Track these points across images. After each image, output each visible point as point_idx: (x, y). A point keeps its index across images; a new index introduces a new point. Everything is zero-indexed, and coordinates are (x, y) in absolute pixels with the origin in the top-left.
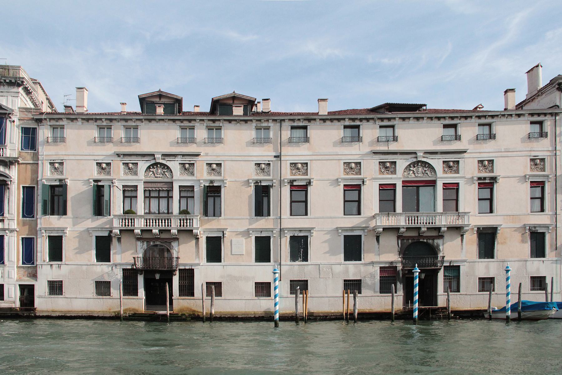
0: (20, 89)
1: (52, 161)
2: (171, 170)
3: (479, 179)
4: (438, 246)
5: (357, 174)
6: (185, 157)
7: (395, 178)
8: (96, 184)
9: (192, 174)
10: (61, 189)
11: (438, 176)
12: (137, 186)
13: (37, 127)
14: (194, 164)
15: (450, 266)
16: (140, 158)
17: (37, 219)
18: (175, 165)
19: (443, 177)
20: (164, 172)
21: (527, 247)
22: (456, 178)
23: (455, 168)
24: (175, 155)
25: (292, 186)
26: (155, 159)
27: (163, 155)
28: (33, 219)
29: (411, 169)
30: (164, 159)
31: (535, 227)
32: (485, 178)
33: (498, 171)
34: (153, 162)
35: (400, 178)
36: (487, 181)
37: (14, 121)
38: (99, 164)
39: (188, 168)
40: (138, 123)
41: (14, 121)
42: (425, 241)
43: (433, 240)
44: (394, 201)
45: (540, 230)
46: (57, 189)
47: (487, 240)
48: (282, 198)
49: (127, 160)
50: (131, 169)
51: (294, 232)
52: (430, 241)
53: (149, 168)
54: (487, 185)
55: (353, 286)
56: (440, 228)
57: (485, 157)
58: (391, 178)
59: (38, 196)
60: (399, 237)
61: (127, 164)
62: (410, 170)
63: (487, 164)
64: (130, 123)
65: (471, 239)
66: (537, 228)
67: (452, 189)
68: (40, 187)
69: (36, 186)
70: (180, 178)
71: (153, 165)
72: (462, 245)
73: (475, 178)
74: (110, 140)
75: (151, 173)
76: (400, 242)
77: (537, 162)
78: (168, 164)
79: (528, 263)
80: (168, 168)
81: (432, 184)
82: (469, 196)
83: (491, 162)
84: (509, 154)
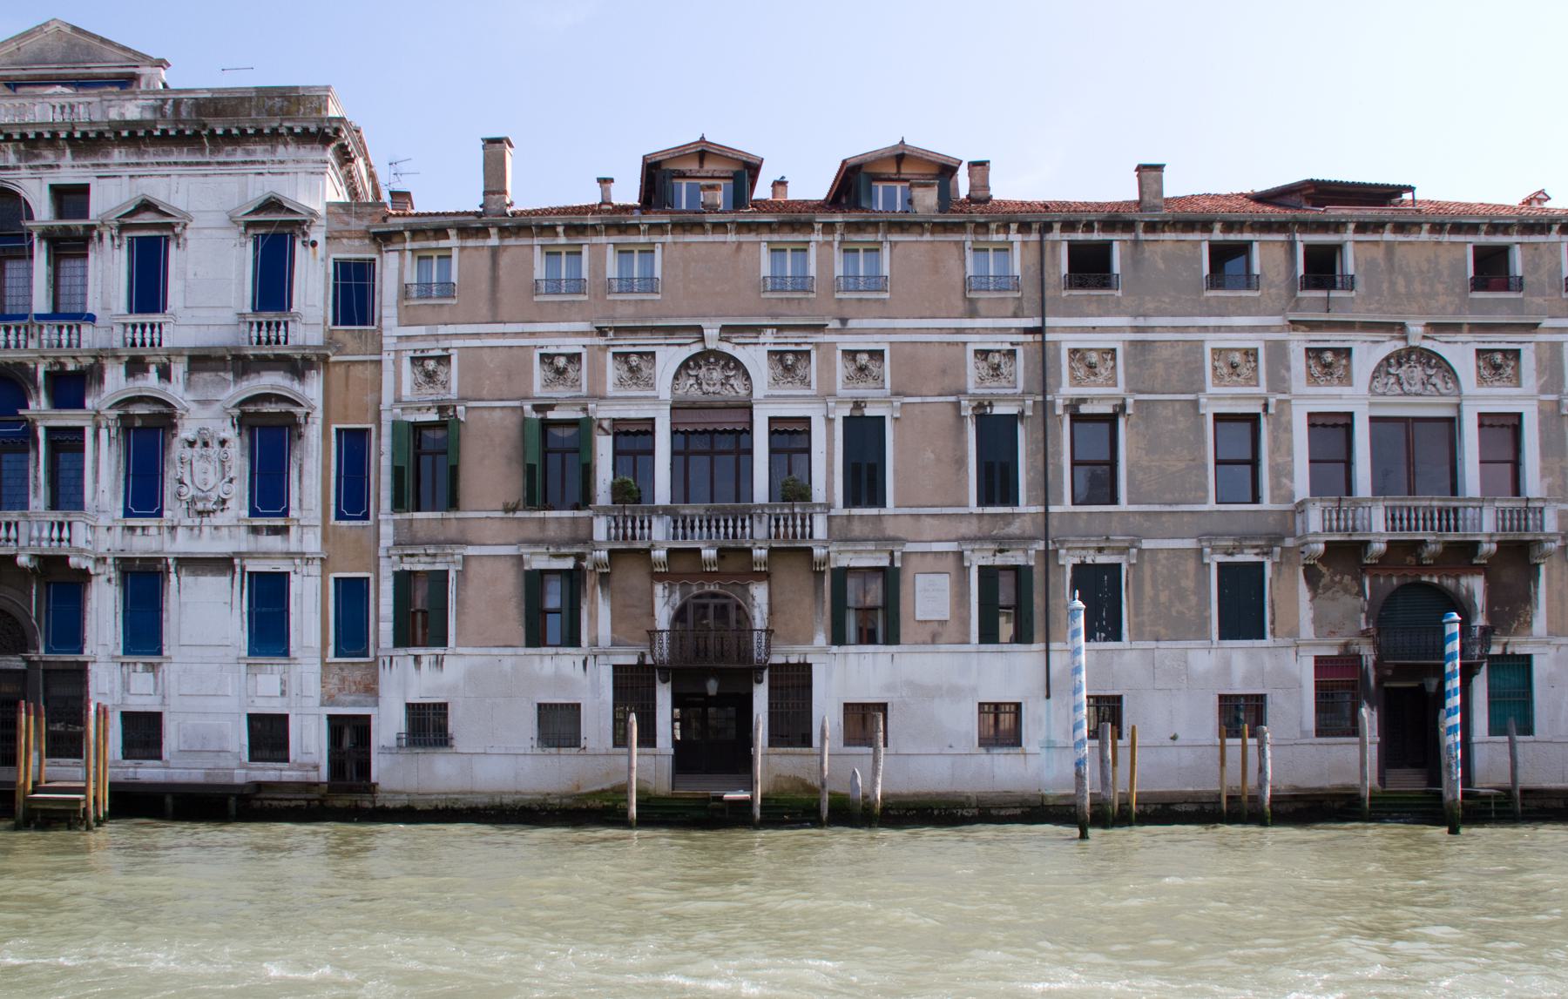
0: (329, 154)
1: (418, 354)
4: (1471, 594)
5: (1247, 385)
6: (786, 334)
8: (540, 416)
9: (805, 382)
10: (439, 434)
12: (653, 419)
13: (377, 256)
14: (808, 353)
15: (1504, 656)
17: (378, 522)
18: (755, 357)
20: (728, 378)
23: (1509, 371)
26: (702, 340)
27: (724, 328)
28: (366, 523)
29: (1392, 370)
30: (727, 340)
34: (697, 348)
37: (314, 244)
41: (314, 244)
42: (1436, 580)
43: (1457, 577)
44: (1348, 463)
46: (429, 434)
49: (625, 344)
51: (1084, 553)
53: (685, 365)
56: (1479, 542)
58: (1340, 397)
59: (380, 454)
61: (627, 355)
62: (1388, 373)
68: (386, 430)
69: (373, 426)
71: (693, 357)
75: (692, 381)
78: (738, 353)
80: (739, 365)
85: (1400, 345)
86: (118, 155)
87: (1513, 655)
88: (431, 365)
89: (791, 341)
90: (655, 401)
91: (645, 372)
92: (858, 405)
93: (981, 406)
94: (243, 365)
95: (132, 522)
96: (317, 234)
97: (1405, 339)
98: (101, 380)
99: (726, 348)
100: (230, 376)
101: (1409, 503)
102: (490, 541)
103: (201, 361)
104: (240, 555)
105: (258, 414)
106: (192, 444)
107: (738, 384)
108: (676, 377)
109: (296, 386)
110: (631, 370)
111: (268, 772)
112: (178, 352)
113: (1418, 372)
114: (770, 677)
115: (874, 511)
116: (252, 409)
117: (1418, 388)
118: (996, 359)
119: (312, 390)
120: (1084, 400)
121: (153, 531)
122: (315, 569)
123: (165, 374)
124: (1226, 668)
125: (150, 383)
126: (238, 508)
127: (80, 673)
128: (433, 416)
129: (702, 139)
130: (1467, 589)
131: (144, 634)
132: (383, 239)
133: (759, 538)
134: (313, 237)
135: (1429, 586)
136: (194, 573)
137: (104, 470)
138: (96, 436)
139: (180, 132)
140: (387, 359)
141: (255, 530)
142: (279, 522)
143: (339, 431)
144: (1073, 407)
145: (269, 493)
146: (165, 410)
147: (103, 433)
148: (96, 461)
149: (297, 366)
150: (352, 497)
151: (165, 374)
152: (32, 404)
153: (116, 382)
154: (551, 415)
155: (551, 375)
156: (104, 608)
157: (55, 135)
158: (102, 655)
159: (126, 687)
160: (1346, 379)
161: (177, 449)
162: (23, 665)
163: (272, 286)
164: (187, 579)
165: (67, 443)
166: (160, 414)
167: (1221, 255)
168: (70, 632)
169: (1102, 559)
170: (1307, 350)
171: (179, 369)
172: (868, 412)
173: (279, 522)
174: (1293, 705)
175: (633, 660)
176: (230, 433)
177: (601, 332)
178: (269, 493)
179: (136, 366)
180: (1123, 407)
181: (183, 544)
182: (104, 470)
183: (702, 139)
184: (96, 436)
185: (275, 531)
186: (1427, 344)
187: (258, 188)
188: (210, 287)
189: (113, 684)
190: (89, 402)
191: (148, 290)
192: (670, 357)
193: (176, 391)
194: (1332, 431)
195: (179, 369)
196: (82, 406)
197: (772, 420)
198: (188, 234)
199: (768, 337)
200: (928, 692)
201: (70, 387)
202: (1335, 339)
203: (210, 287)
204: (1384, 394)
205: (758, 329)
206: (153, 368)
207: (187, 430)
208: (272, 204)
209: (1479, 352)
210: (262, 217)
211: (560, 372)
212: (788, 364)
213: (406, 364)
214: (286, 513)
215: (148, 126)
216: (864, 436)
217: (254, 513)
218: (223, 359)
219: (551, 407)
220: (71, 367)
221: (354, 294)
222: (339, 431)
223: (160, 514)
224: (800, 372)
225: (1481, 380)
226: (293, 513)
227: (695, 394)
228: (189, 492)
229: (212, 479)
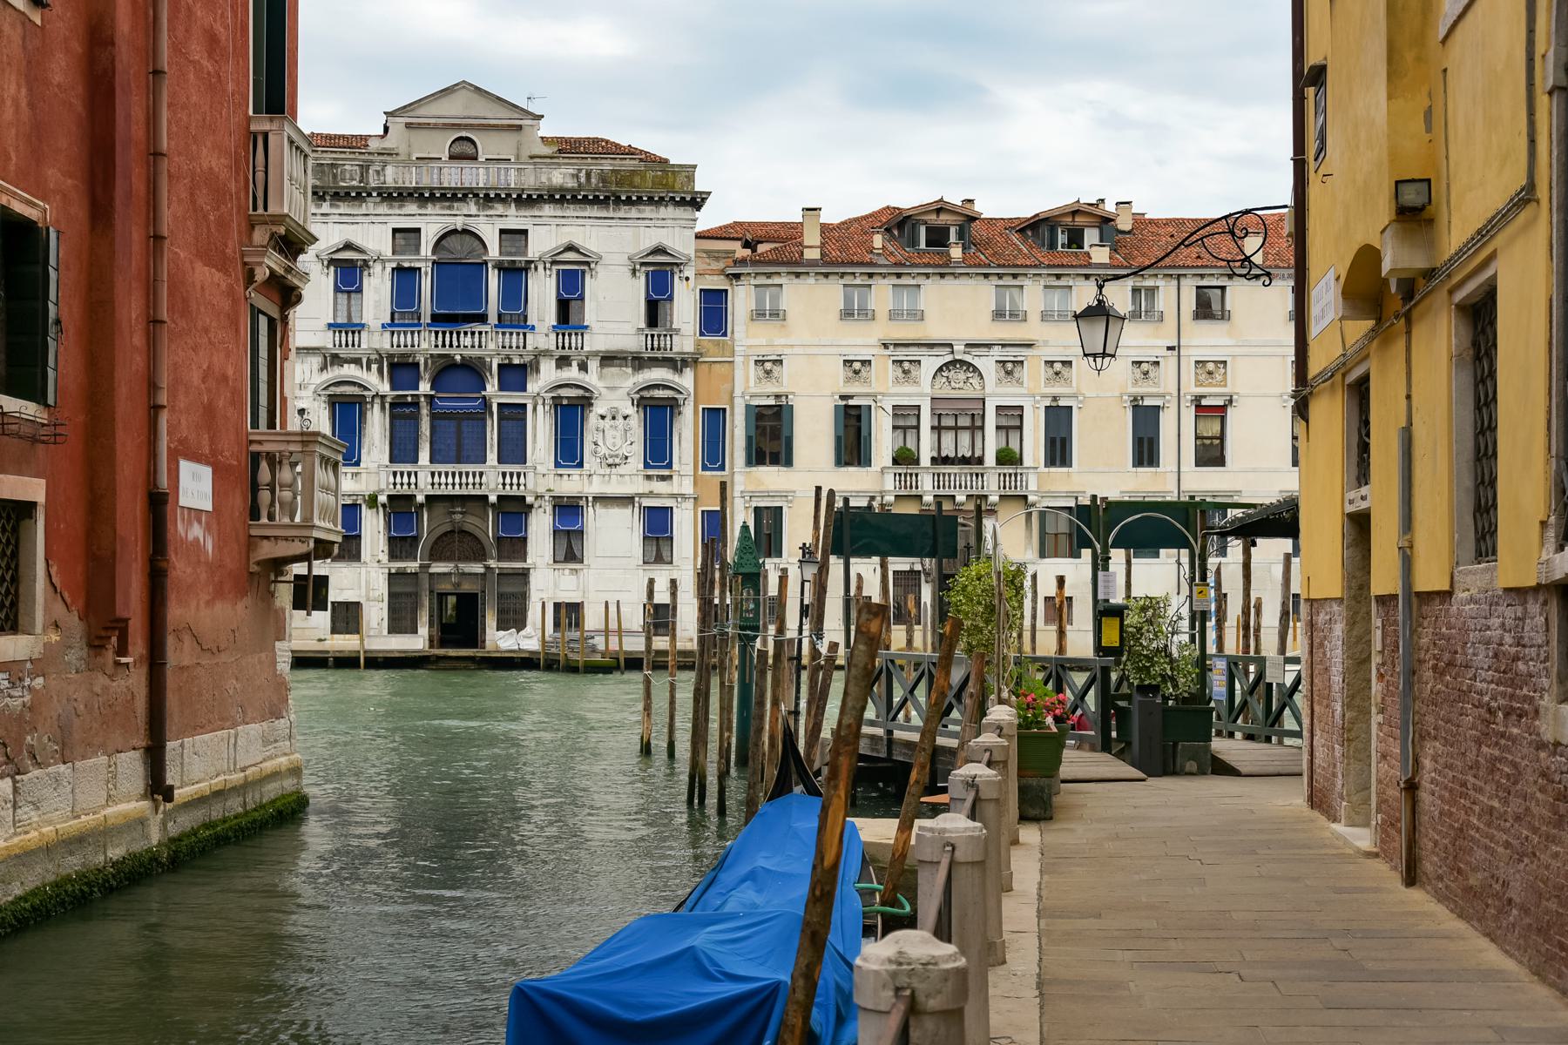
2: (980, 375)
9: (1019, 382)
16: (924, 351)
18: (986, 363)
24: (989, 346)
25: (1199, 407)
27: (967, 345)
34: (949, 358)
39: (1009, 369)
49: (901, 354)
50: (906, 369)
53: (940, 369)
61: (901, 362)
64: (905, 281)
70: (997, 393)
74: (867, 315)
78: (976, 362)
80: (975, 369)
86: (548, 210)
88: (768, 366)
89: (1010, 354)
90: (922, 390)
91: (914, 373)
92: (1055, 399)
93: (1135, 399)
94: (639, 362)
95: (561, 471)
96: (689, 272)
98: (538, 371)
99: (968, 358)
100: (629, 370)
103: (608, 359)
104: (641, 496)
105: (651, 398)
106: (603, 417)
107: (975, 381)
109: (676, 378)
110: (905, 372)
111: (661, 643)
112: (595, 354)
115: (1065, 470)
116: (646, 394)
118: (1145, 367)
119: (686, 380)
121: (576, 478)
122: (690, 504)
123: (583, 367)
125: (572, 373)
126: (636, 463)
127: (524, 575)
131: (570, 547)
133: (992, 486)
134: (686, 274)
136: (605, 506)
137: (541, 432)
138: (535, 409)
139: (596, 197)
140: (738, 360)
141: (649, 477)
142: (666, 472)
144: (1197, 399)
145: (658, 452)
146: (580, 392)
147: (540, 408)
148: (535, 428)
149: (677, 364)
150: (713, 454)
151: (583, 367)
152: (488, 387)
153: (548, 374)
154: (851, 402)
155: (851, 374)
156: (540, 527)
157: (509, 195)
158: (540, 563)
159: (556, 585)
161: (592, 420)
162: (482, 570)
163: (655, 312)
164: (600, 510)
165: (514, 416)
166: (584, 397)
168: (516, 546)
171: (593, 365)
172: (1062, 403)
173: (666, 472)
175: (907, 568)
176: (631, 410)
177: (886, 346)
178: (658, 452)
179: (563, 362)
180: (1231, 401)
181: (596, 487)
182: (541, 432)
184: (535, 409)
185: (663, 478)
187: (649, 237)
188: (614, 309)
189: (548, 582)
190: (529, 387)
191: (567, 311)
192: (930, 363)
193: (593, 378)
195: (593, 365)
196: (525, 390)
198: (599, 268)
199: (996, 351)
201: (515, 374)
203: (614, 309)
205: (989, 346)
206: (575, 364)
207: (599, 408)
208: (659, 250)
210: (651, 259)
211: (856, 372)
212: (1009, 369)
213: (752, 363)
214: (670, 466)
215: (563, 190)
216: (1059, 420)
217: (646, 466)
218: (625, 359)
219: (851, 397)
220: (516, 361)
221: (714, 312)
223: (581, 465)
224: (1016, 375)
226: (675, 467)
227: (947, 392)
228: (603, 450)
229: (619, 442)
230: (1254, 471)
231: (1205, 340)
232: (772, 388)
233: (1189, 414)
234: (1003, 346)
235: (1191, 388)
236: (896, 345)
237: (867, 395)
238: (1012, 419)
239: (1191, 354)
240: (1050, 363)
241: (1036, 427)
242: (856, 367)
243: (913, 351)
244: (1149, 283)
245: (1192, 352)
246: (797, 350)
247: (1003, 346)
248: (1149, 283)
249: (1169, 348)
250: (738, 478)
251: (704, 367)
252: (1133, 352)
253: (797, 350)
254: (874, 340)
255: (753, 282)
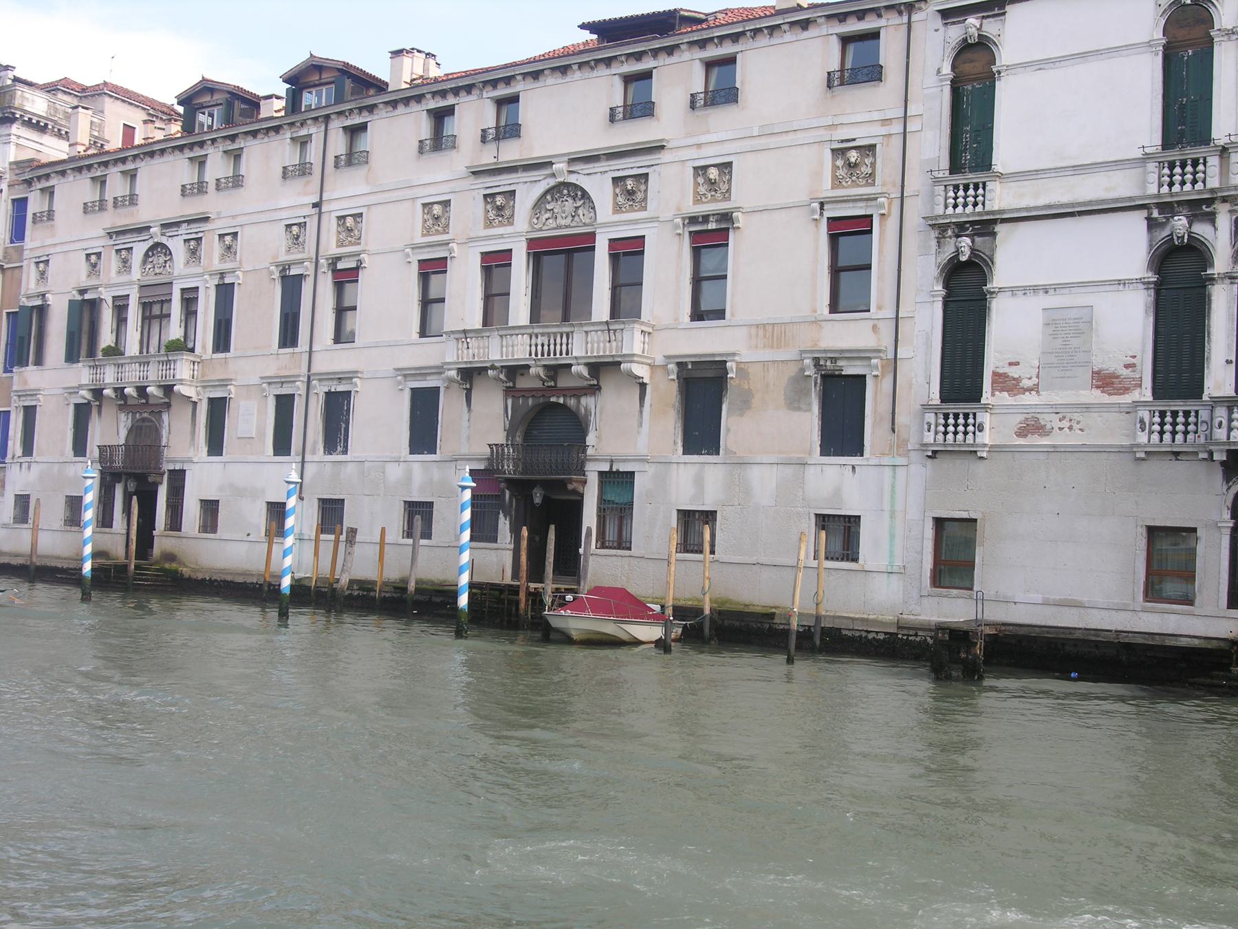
3: (693, 220)
7: (510, 236)
11: (600, 220)
15: (610, 472)
18: (177, 245)
19: (609, 221)
21: (809, 422)
22: (635, 222)
24: (177, 224)
25: (335, 272)
31: (834, 360)
32: (706, 218)
33: (744, 193)
34: (151, 243)
35: (519, 234)
36: (712, 226)
38: (88, 256)
39: (194, 247)
40: (138, 164)
42: (561, 401)
43: (578, 397)
45: (850, 369)
47: (703, 397)
48: (320, 300)
51: (330, 383)
52: (572, 402)
53: (146, 255)
54: (709, 237)
55: (419, 514)
57: (710, 155)
58: (502, 236)
60: (509, 392)
63: (715, 176)
64: (130, 166)
65: (665, 392)
66: (840, 363)
67: (628, 253)
72: (641, 412)
73: (679, 221)
76: (510, 402)
77: (853, 158)
78: (170, 243)
79: (811, 472)
81: (585, 243)
82: (667, 271)
83: (726, 167)
84: (773, 142)
85: (552, 182)
87: (618, 472)
92: (222, 275)
93: (284, 270)
97: (553, 175)
99: (164, 240)
101: (560, 330)
102: (54, 381)
108: (144, 262)
113: (569, 205)
114: (169, 479)
117: (570, 218)
120: (339, 259)
124: (408, 478)
128: (39, 302)
129: (204, 79)
130: (586, 409)
132: (29, 182)
135: (564, 406)
143: (8, 314)
154: (87, 297)
160: (510, 220)
167: (440, 116)
169: (341, 388)
170: (485, 196)
172: (227, 281)
174: (456, 514)
177: (110, 235)
183: (204, 79)
186: (572, 179)
192: (140, 250)
194: (495, 264)
197: (182, 290)
199: (183, 229)
200: (239, 492)
202: (503, 182)
204: (541, 230)
205: (177, 224)
209: (616, 180)
212: (194, 247)
213: (33, 267)
222: (8, 314)
225: (618, 209)
230: (377, 346)
231: (346, 191)
232: (42, 289)
233: (326, 285)
234: (189, 222)
235: (331, 247)
236: (119, 233)
237: (96, 288)
238: (190, 299)
239: (333, 209)
240: (221, 236)
241: (206, 308)
242: (93, 261)
243: (128, 238)
244: (304, 132)
245: (334, 206)
246: (58, 249)
247: (189, 222)
248: (304, 132)
249: (315, 205)
250: (16, 378)
251: (9, 273)
252: (284, 214)
253: (58, 249)
254: (102, 233)
255: (40, 186)
